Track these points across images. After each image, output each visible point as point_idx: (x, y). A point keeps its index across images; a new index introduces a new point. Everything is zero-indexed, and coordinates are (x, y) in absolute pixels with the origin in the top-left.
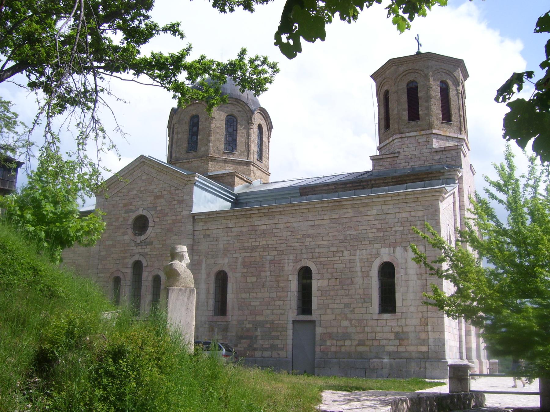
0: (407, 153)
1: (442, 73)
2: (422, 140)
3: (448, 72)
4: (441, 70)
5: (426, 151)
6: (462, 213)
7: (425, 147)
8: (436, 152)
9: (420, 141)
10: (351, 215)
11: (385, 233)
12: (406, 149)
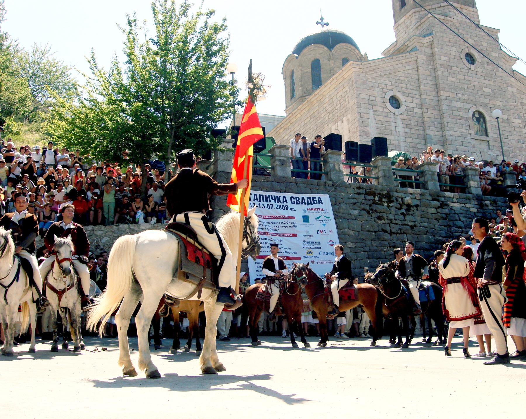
0: (401, 39)
6: (436, 75)
8: (417, 28)
10: (317, 108)
11: (334, 113)
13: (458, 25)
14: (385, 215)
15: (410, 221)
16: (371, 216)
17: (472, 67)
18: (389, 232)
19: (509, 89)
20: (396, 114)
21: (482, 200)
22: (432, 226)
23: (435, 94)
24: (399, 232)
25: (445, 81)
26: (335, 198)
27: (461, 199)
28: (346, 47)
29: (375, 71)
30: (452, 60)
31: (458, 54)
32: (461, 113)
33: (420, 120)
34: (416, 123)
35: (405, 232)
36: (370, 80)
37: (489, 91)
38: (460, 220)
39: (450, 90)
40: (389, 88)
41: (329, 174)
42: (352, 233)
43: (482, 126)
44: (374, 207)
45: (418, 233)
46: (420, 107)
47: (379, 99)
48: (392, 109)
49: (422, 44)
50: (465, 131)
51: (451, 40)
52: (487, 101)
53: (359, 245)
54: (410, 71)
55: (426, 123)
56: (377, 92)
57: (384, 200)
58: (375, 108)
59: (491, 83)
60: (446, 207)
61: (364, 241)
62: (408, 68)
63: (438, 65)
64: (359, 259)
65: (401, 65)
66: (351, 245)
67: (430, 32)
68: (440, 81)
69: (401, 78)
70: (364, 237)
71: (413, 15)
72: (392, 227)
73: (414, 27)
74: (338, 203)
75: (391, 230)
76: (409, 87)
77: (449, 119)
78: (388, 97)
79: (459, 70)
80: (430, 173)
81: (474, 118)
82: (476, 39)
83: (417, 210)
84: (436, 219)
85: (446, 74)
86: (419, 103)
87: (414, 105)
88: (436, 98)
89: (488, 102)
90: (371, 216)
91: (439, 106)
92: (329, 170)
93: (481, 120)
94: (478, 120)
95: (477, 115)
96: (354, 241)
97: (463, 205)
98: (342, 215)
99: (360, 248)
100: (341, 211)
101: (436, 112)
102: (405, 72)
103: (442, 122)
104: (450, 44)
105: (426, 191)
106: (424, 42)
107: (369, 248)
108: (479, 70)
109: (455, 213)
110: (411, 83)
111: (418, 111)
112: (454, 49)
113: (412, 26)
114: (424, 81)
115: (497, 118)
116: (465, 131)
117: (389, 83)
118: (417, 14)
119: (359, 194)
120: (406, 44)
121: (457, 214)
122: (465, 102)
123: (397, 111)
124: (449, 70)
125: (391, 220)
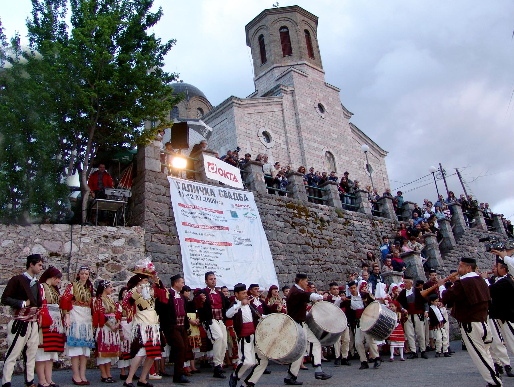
0: (262, 89)
1: (281, 21)
2: (269, 75)
3: (286, 19)
4: (280, 19)
5: (272, 82)
6: (297, 119)
7: (271, 79)
9: (268, 76)
12: (262, 86)
13: (311, 80)
14: (306, 228)
15: (326, 235)
16: (295, 229)
17: (323, 115)
18: (311, 245)
19: (348, 137)
20: (268, 147)
21: (373, 219)
22: (343, 241)
23: (296, 134)
24: (320, 245)
25: (304, 124)
26: (261, 209)
27: (359, 218)
28: (200, 100)
29: (250, 108)
30: (308, 108)
31: (313, 104)
32: (317, 152)
33: (286, 154)
34: (283, 157)
35: (324, 245)
36: (247, 115)
37: (335, 136)
38: (361, 237)
39: (309, 132)
40: (262, 124)
41: (252, 185)
42: (281, 245)
43: (332, 165)
44: (296, 220)
45: (334, 247)
46: (285, 143)
47: (254, 133)
48: (265, 143)
49: (285, 92)
50: (320, 167)
51: (307, 91)
52: (334, 144)
53: (289, 258)
54: (277, 113)
55: (291, 157)
56: (252, 127)
57: (302, 213)
58: (251, 140)
59: (337, 130)
60: (349, 224)
61: (292, 254)
62: (275, 110)
63: (299, 111)
64: (291, 272)
65: (270, 107)
66: (282, 257)
67: (291, 83)
68: (301, 124)
69: (271, 118)
70: (291, 250)
71: (275, 69)
72: (313, 241)
73: (276, 79)
74: (265, 214)
75: (313, 244)
76: (276, 125)
77: (309, 156)
78: (261, 132)
79: (314, 116)
80: (333, 191)
81: (327, 158)
82: (324, 94)
83: (329, 225)
84: (344, 235)
85: (305, 119)
86: (285, 140)
87: (280, 142)
88: (297, 138)
89: (335, 145)
90: (295, 229)
91: (300, 145)
92: (251, 180)
93: (331, 159)
94: (329, 159)
95: (328, 155)
96: (284, 253)
97: (360, 223)
98: (271, 226)
99: (290, 261)
100: (269, 222)
101: (298, 149)
102: (273, 113)
103: (304, 157)
104: (306, 95)
105: (332, 208)
106: (287, 90)
107: (298, 261)
108: (328, 118)
109: (356, 230)
110: (279, 123)
111: (284, 147)
112: (310, 99)
113: (273, 78)
114: (288, 122)
115: (366, 152)
116: (320, 167)
117: (261, 120)
118: (278, 68)
119: (281, 206)
120: (272, 91)
121: (358, 231)
122: (319, 143)
123: (269, 145)
124: (307, 116)
125: (311, 233)
